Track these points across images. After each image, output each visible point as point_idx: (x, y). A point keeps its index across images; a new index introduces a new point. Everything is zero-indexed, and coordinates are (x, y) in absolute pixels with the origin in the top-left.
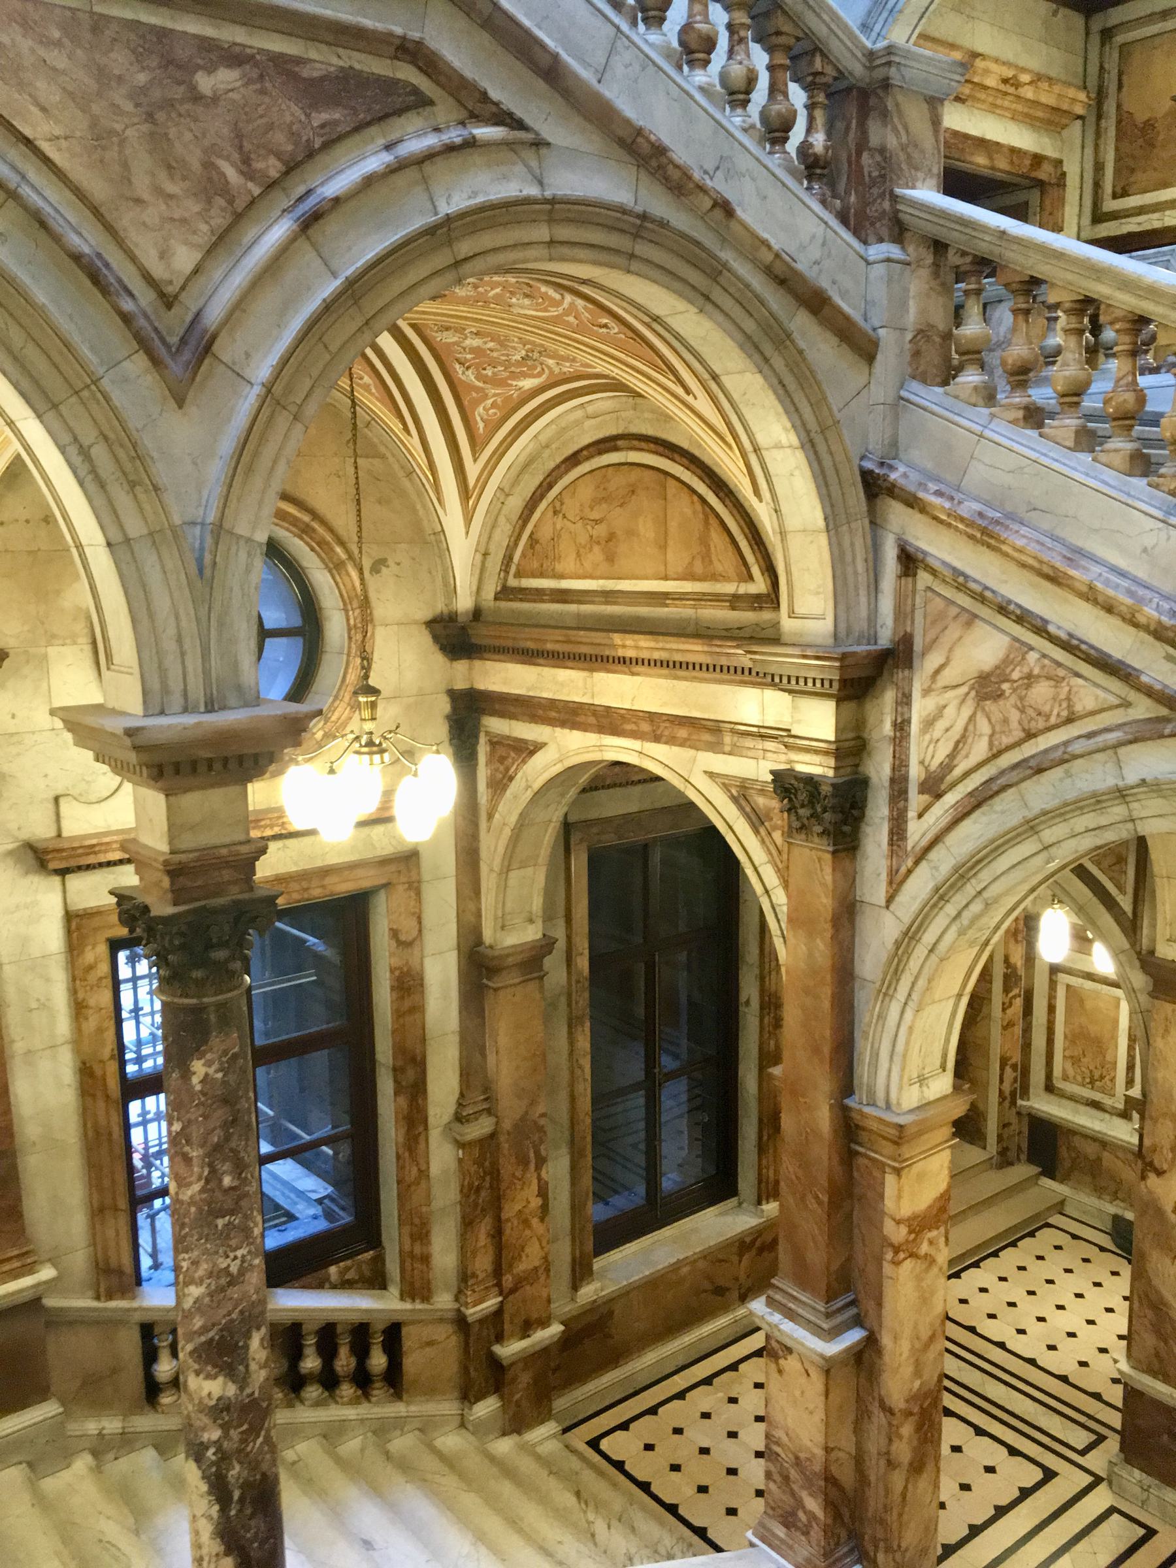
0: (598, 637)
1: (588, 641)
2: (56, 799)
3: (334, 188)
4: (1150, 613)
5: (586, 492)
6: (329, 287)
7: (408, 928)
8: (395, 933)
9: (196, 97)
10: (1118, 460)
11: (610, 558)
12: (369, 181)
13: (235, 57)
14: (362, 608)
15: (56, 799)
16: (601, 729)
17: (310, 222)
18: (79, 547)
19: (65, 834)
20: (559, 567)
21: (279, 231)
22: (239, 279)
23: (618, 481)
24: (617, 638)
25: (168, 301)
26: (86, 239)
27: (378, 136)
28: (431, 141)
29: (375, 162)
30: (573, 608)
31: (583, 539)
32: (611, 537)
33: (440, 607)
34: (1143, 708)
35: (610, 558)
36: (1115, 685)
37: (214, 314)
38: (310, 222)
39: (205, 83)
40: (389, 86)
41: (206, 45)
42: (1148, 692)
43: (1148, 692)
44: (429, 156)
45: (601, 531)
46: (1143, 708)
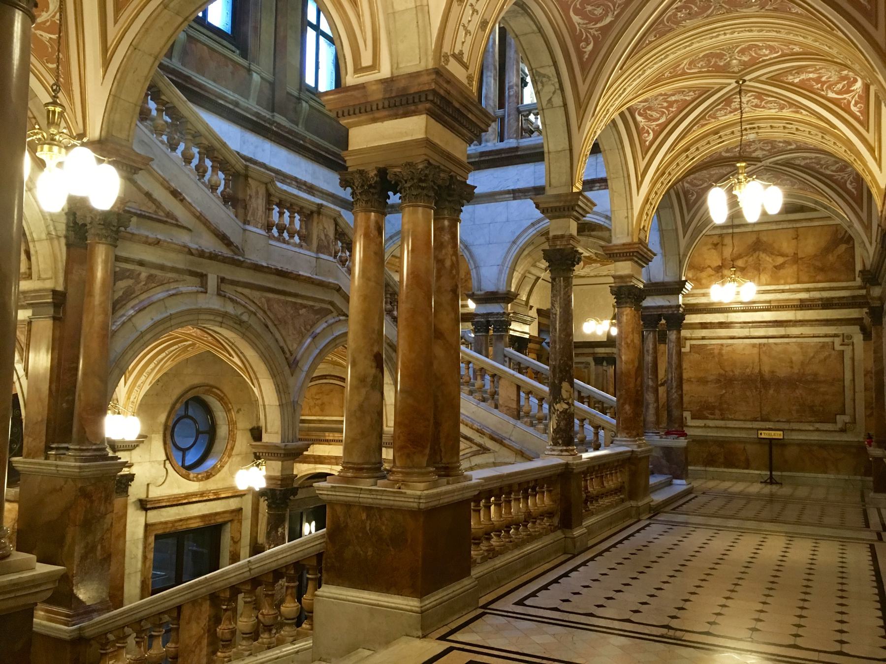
0: (321, 434)
1: (314, 435)
2: (148, 485)
3: (318, 331)
4: (475, 426)
5: (314, 390)
6: (317, 351)
7: (237, 535)
8: (232, 538)
9: (299, 315)
10: (467, 392)
11: (322, 410)
12: (324, 329)
13: (305, 307)
14: (232, 424)
15: (148, 485)
16: (316, 463)
17: (314, 338)
18: (264, 406)
19: (150, 496)
20: (302, 412)
21: (309, 340)
22: (303, 350)
23: (328, 387)
24: (327, 434)
25: (291, 355)
26: (282, 344)
27: (324, 320)
28: (333, 321)
29: (325, 325)
30: (306, 425)
31: (312, 404)
32: (323, 404)
33: (254, 425)
34: (475, 448)
35: (322, 410)
36: (468, 443)
37: (298, 358)
38: (314, 338)
39: (301, 312)
40: (327, 309)
41: (301, 304)
42: (476, 444)
43: (476, 444)
44: (333, 324)
45: (319, 402)
46: (475, 448)
